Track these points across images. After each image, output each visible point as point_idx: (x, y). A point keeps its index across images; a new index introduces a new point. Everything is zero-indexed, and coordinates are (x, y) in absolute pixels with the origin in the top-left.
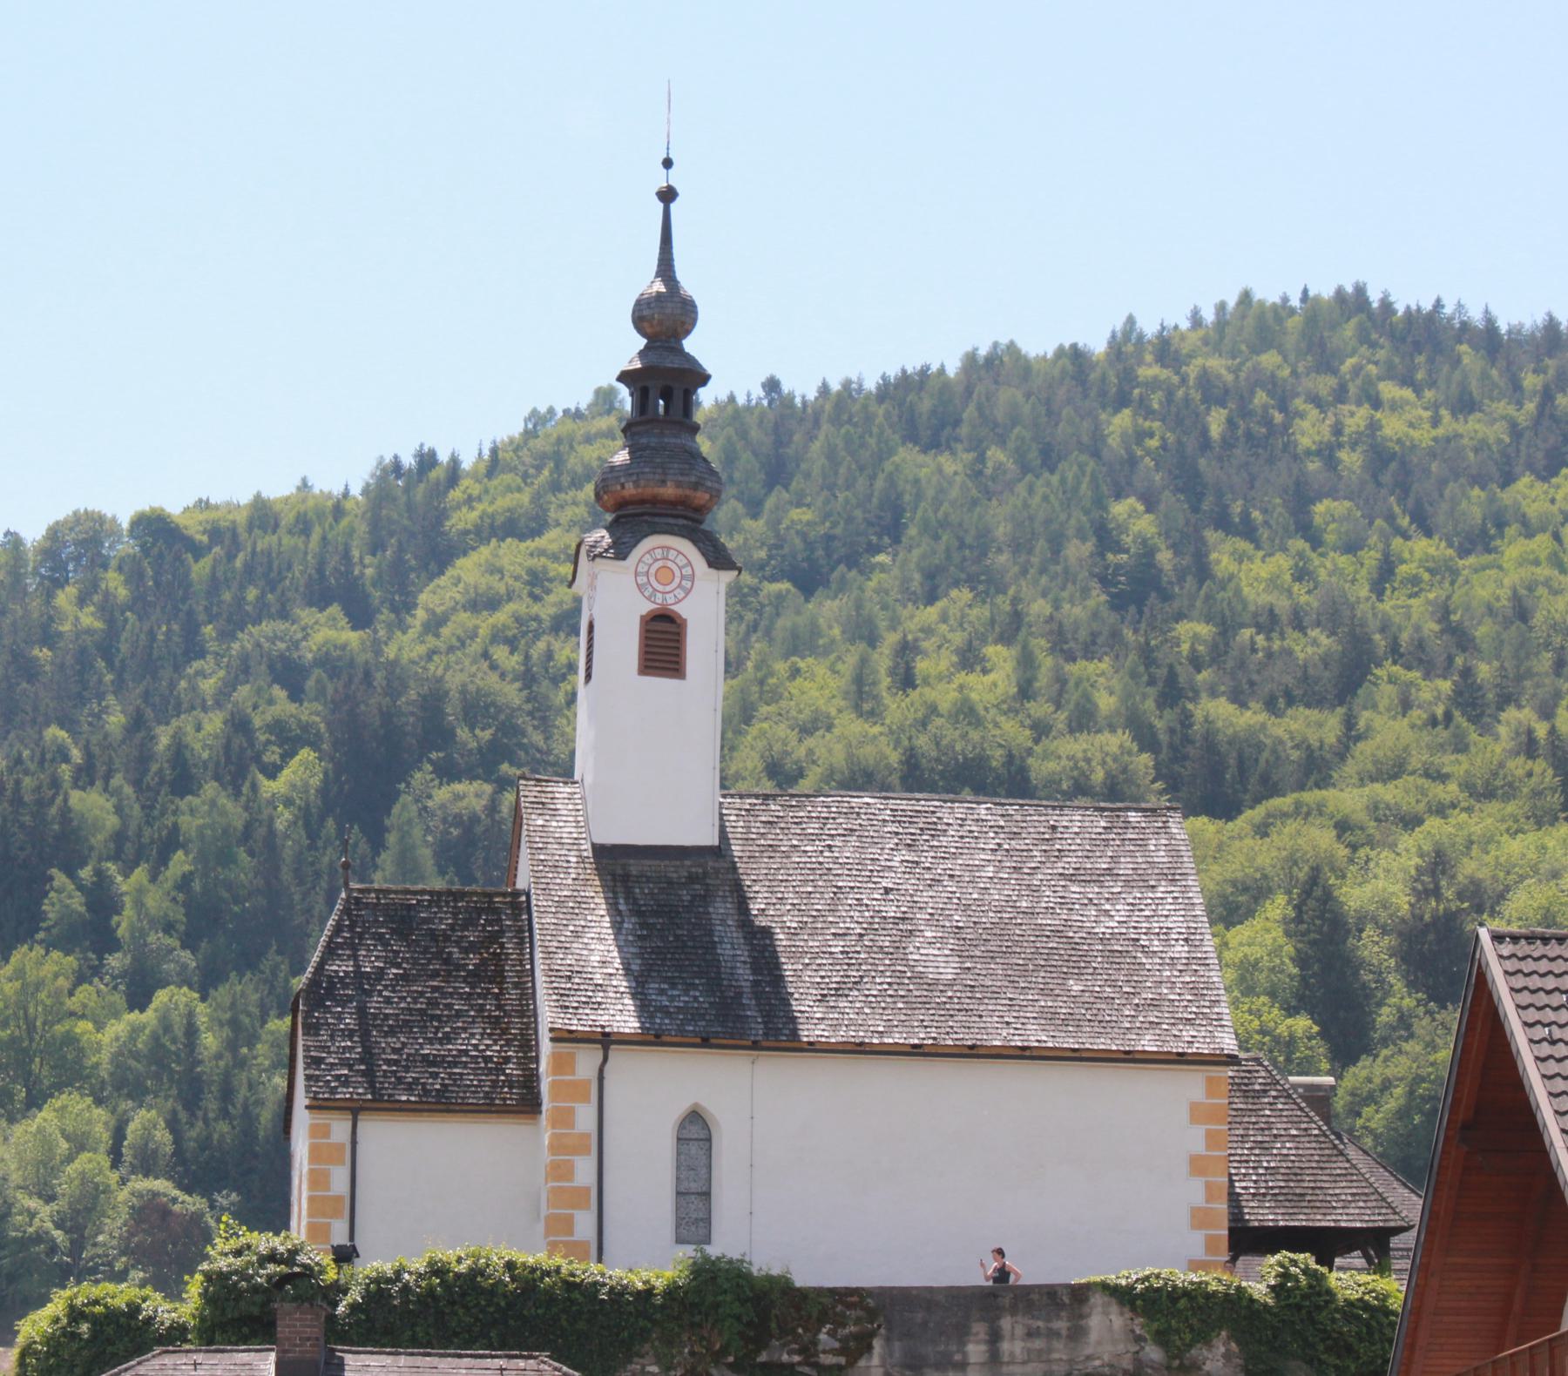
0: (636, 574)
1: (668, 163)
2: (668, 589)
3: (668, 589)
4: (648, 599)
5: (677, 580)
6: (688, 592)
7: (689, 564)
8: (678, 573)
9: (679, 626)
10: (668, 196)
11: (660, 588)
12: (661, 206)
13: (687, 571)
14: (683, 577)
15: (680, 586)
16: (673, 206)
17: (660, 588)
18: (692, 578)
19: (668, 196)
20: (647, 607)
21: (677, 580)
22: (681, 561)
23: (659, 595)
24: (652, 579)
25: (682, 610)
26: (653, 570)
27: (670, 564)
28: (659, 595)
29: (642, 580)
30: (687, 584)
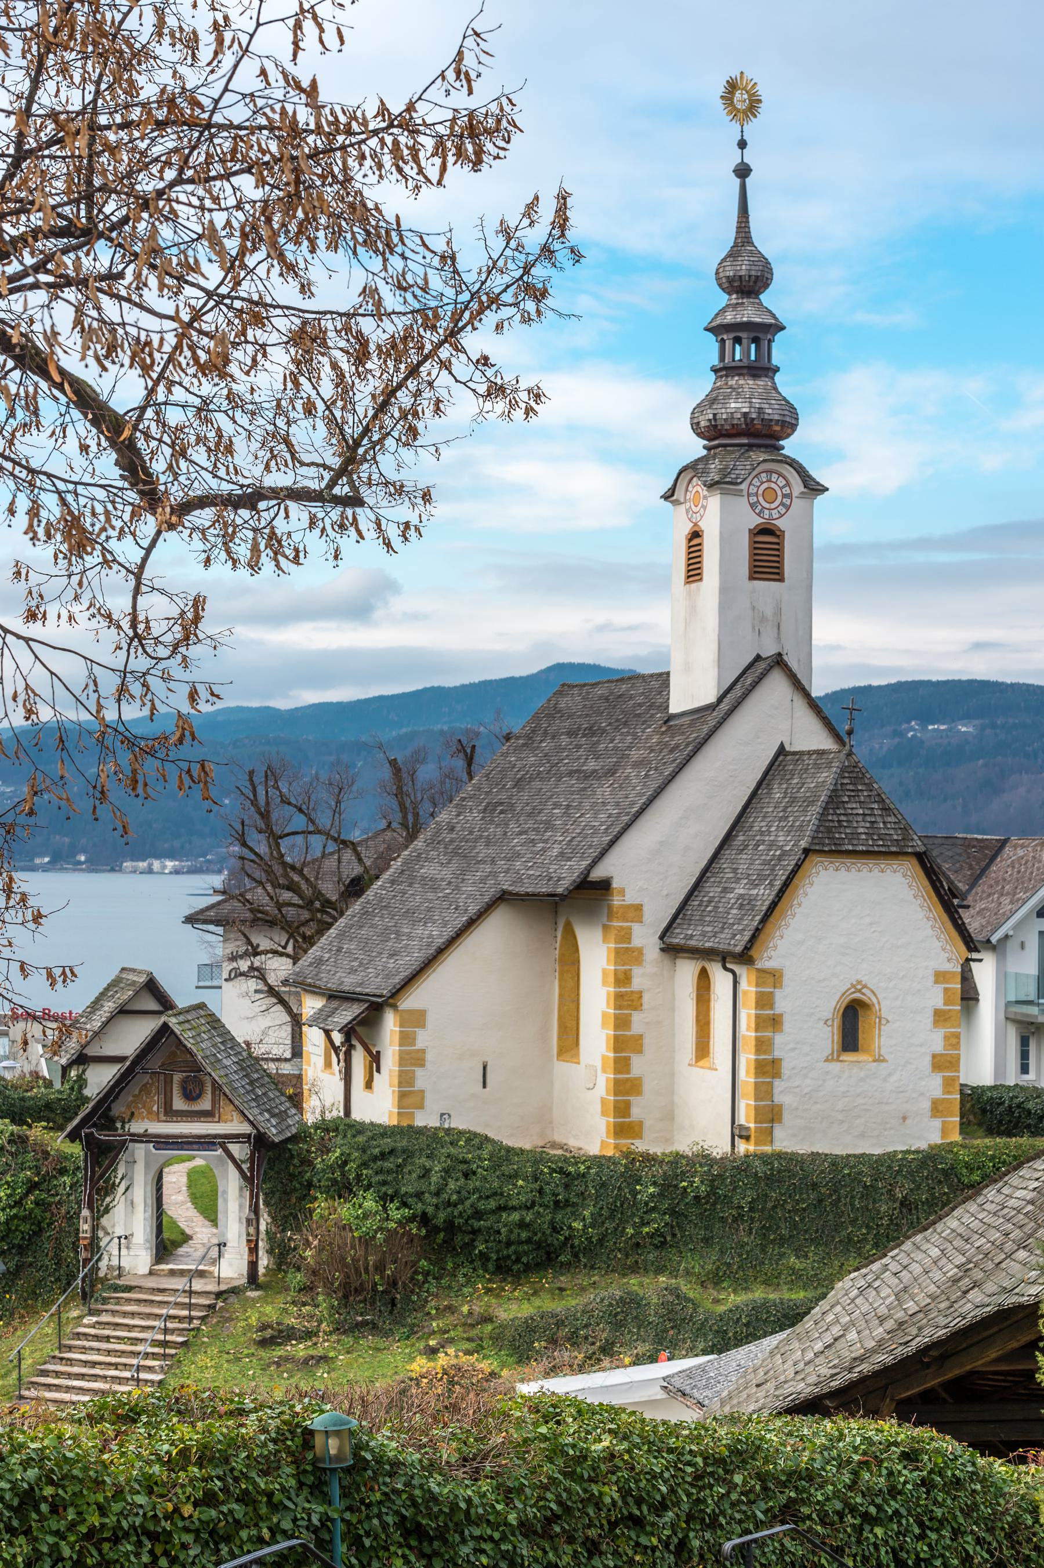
0: (749, 495)
1: (742, 144)
2: (773, 506)
3: (773, 506)
4: (758, 515)
5: (779, 498)
6: (788, 508)
7: (788, 484)
8: (779, 493)
9: (778, 536)
10: (743, 172)
11: (766, 505)
12: (738, 181)
13: (786, 490)
14: (784, 496)
15: (782, 504)
16: (747, 180)
17: (766, 505)
18: (789, 496)
19: (743, 172)
20: (756, 521)
21: (779, 498)
22: (781, 482)
23: (766, 512)
24: (761, 499)
25: (780, 523)
26: (760, 492)
27: (773, 485)
28: (766, 512)
29: (753, 499)
30: (787, 501)
